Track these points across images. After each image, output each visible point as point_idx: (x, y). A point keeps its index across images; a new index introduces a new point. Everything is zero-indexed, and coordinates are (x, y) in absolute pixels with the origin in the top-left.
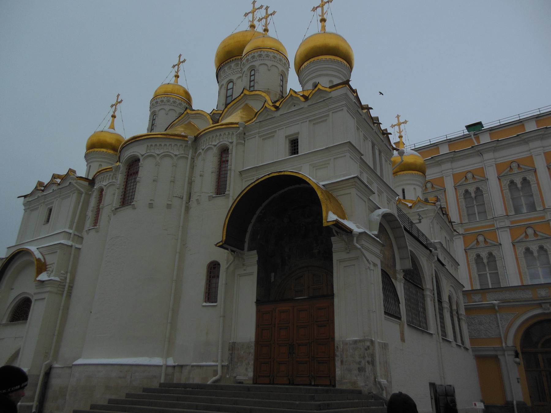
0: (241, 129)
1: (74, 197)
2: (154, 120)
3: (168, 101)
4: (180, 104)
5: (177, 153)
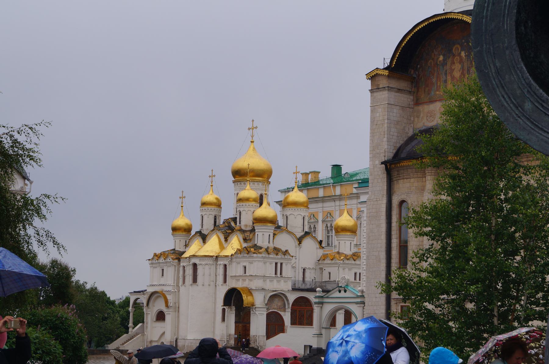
0: (230, 259)
1: (173, 267)
4: (214, 210)
5: (210, 263)
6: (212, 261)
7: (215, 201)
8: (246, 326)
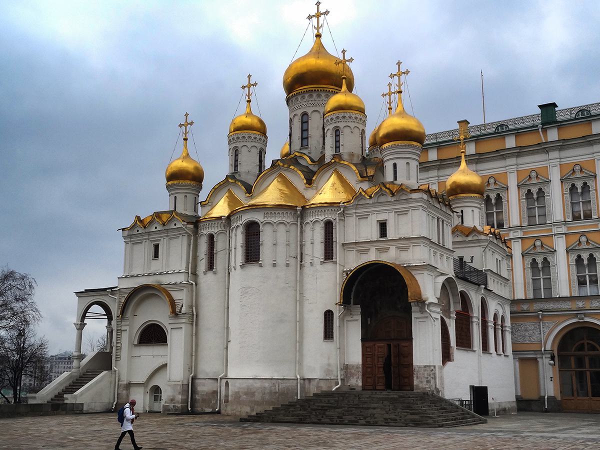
0: (342, 209)
1: (185, 239)
2: (236, 155)
3: (250, 137)
6: (291, 217)
7: (259, 125)
8: (398, 345)
